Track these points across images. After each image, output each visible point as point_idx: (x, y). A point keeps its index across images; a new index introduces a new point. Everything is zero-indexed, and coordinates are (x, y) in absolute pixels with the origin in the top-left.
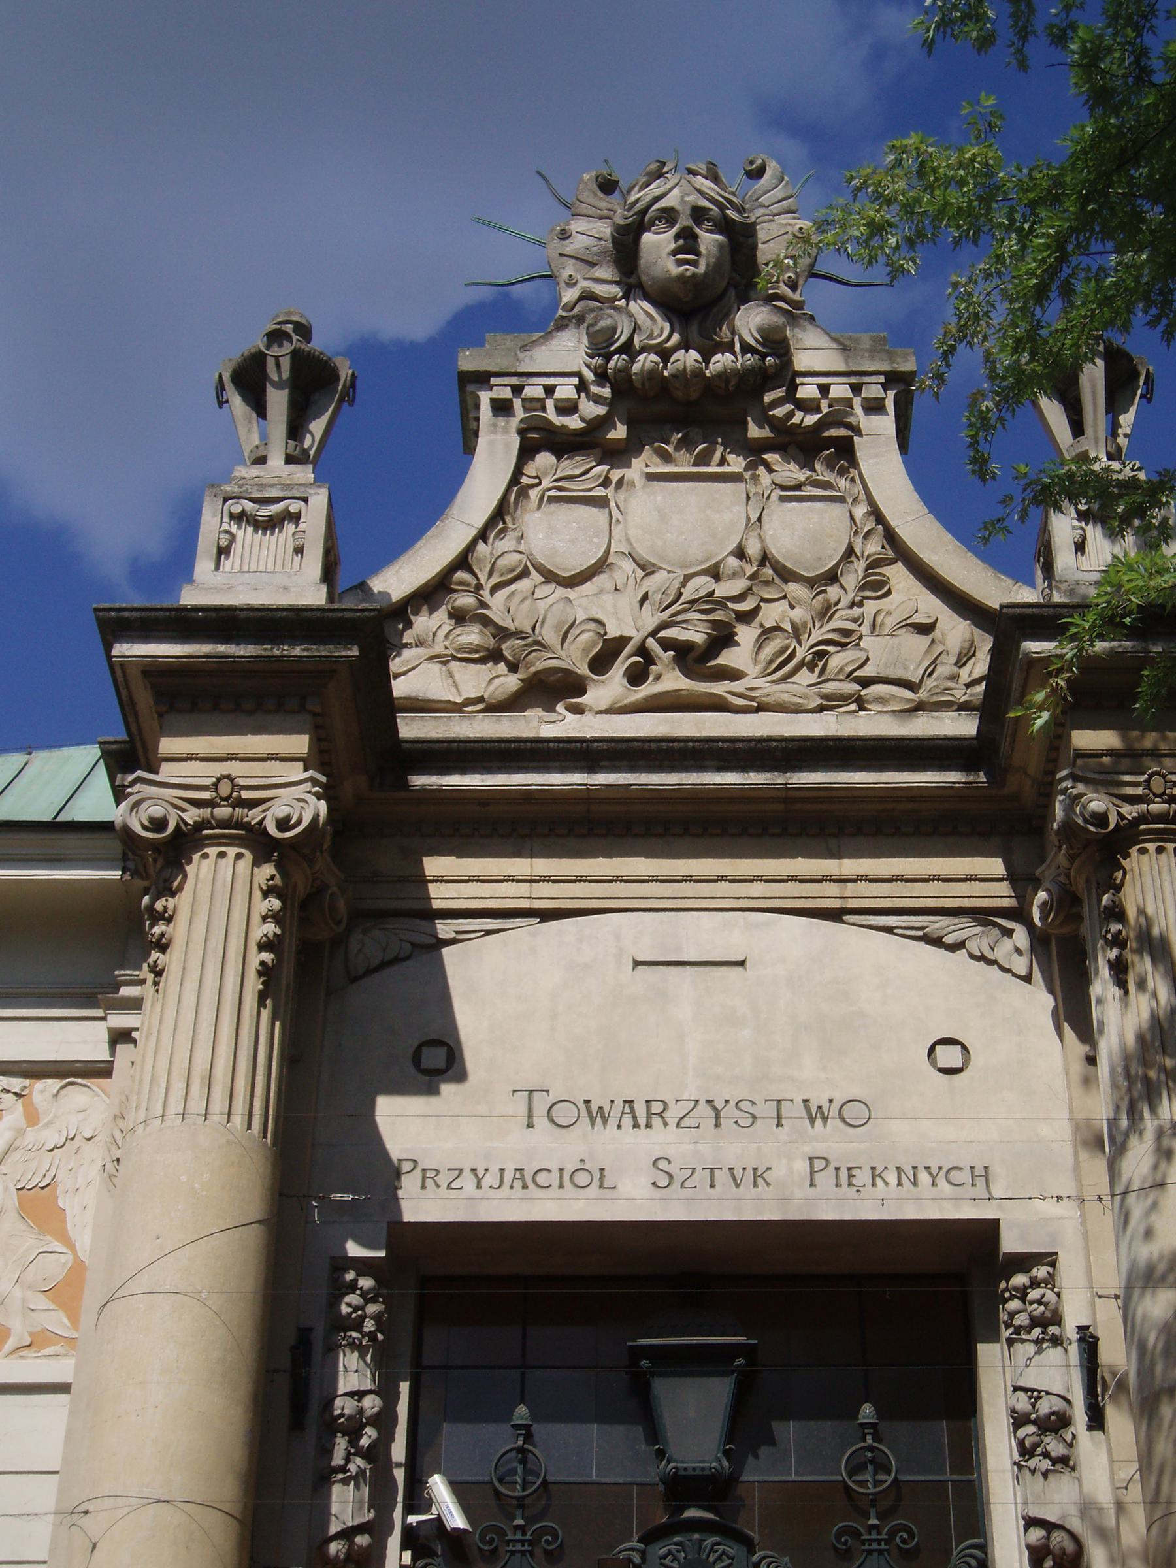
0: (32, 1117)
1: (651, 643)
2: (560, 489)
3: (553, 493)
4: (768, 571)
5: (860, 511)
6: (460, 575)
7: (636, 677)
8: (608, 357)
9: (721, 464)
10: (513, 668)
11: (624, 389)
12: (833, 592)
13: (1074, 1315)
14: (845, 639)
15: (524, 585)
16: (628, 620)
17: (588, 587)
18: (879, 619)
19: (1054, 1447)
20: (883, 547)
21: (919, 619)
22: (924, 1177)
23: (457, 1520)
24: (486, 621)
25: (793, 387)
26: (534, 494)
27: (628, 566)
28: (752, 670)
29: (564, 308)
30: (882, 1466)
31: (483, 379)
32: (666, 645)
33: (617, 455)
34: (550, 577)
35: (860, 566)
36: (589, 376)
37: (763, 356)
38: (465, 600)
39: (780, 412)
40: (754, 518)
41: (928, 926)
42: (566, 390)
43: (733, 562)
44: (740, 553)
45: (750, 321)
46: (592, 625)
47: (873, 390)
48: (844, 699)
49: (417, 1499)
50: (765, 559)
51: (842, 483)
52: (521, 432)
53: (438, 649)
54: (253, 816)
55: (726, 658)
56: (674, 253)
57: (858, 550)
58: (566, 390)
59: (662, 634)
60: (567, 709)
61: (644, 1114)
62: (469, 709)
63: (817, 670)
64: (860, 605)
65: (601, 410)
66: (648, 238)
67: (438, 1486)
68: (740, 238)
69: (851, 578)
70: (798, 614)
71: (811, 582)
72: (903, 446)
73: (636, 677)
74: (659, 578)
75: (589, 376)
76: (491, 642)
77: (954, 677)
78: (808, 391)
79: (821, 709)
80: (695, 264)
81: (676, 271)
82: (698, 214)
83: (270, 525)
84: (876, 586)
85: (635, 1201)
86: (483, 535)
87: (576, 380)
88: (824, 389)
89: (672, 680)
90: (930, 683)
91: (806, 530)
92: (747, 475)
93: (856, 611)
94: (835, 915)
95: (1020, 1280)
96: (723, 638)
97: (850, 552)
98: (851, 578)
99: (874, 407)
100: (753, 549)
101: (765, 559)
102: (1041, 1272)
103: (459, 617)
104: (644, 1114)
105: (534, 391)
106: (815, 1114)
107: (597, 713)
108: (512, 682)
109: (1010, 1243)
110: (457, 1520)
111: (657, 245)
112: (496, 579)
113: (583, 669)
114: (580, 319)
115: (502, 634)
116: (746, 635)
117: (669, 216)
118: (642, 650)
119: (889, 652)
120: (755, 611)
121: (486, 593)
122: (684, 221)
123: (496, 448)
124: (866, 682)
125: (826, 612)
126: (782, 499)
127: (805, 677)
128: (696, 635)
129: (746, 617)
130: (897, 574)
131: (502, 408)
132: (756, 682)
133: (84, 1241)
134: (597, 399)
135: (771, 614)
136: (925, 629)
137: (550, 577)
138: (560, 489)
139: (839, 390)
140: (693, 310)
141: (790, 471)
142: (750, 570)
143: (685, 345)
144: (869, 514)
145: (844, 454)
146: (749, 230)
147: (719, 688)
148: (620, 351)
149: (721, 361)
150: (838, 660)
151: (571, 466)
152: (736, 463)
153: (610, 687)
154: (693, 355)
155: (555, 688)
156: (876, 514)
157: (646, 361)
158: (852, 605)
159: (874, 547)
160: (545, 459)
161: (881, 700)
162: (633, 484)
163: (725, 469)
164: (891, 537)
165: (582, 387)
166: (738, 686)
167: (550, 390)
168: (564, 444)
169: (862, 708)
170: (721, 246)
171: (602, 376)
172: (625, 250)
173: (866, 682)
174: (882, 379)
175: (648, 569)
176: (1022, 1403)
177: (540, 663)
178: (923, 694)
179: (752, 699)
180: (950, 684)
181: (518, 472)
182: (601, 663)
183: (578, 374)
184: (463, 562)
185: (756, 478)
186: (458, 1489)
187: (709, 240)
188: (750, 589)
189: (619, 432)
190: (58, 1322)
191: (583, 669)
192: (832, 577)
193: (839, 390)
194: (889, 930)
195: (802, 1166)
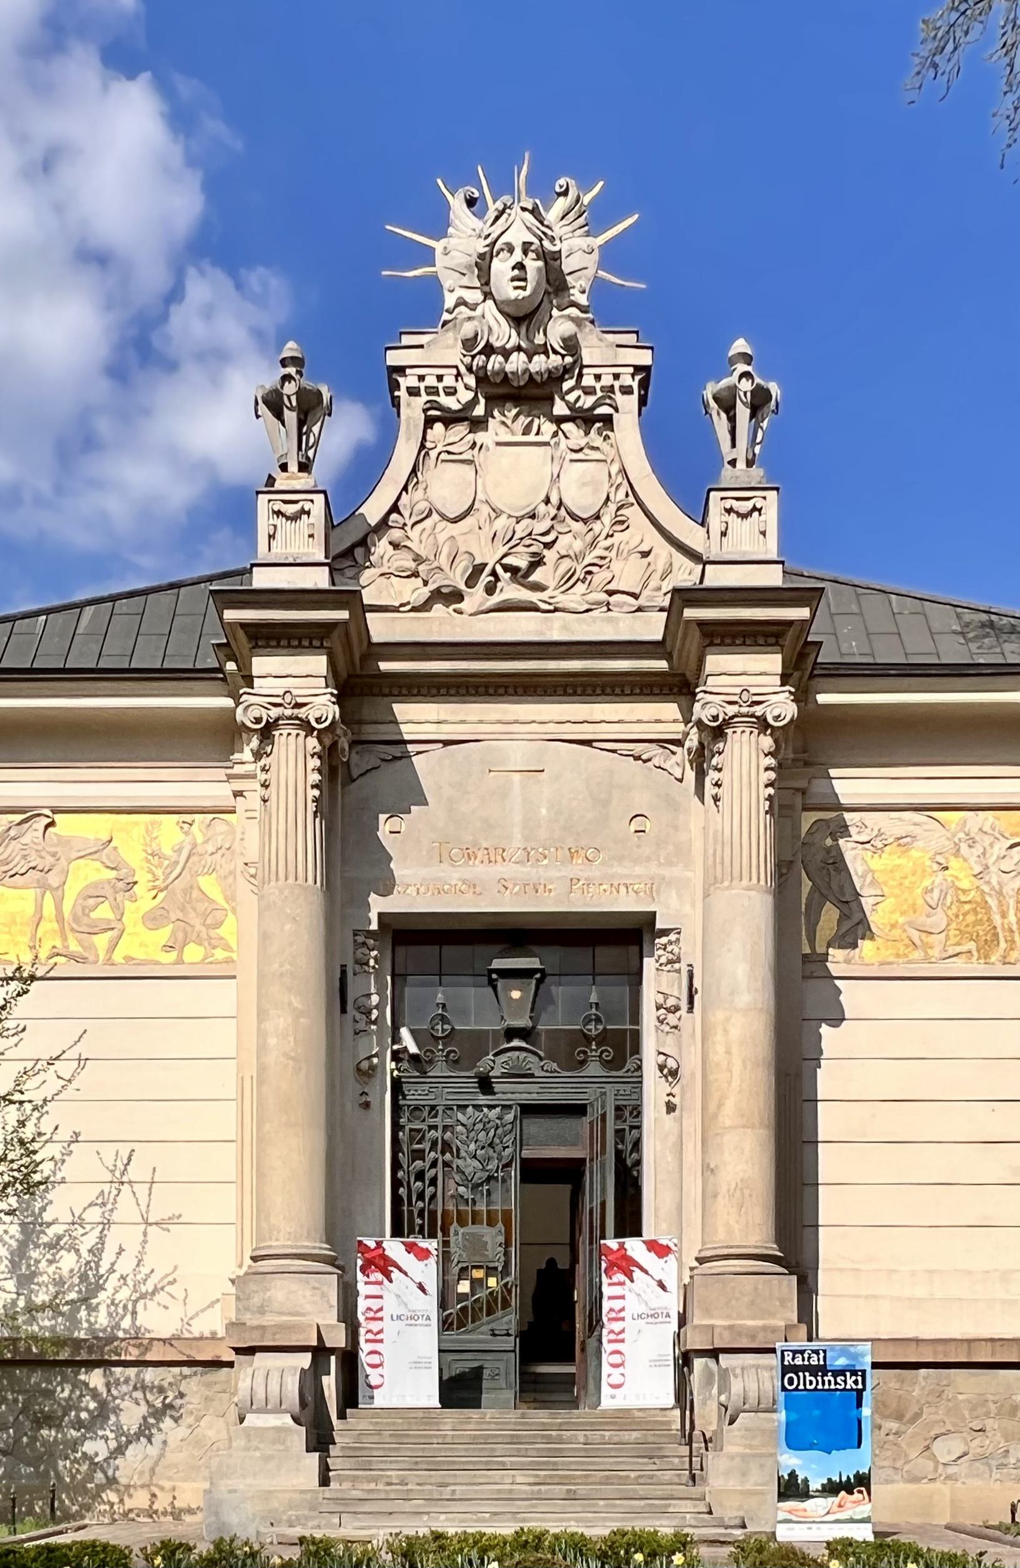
2: (449, 453)
3: (444, 456)
4: (563, 512)
5: (614, 469)
6: (394, 516)
7: (490, 590)
8: (473, 357)
9: (538, 434)
11: (483, 379)
12: (597, 526)
14: (601, 563)
15: (428, 523)
18: (621, 547)
19: (672, 1019)
20: (627, 495)
21: (645, 548)
22: (623, 889)
23: (413, 1049)
25: (580, 375)
26: (433, 454)
27: (485, 510)
28: (552, 584)
29: (447, 311)
30: (598, 1020)
31: (401, 370)
32: (506, 568)
33: (478, 424)
34: (443, 517)
35: (612, 507)
36: (463, 370)
37: (563, 356)
39: (571, 398)
40: (555, 476)
42: (449, 381)
43: (542, 509)
44: (547, 501)
45: (558, 328)
46: (467, 555)
47: (627, 380)
48: (599, 603)
49: (396, 1039)
50: (561, 503)
51: (605, 446)
52: (425, 411)
53: (385, 570)
55: (536, 576)
56: (513, 280)
57: (612, 497)
59: (504, 561)
60: (455, 611)
62: (402, 609)
63: (587, 582)
64: (612, 536)
65: (470, 395)
66: (496, 263)
67: (404, 1032)
68: (551, 260)
69: (607, 519)
70: (578, 545)
71: (585, 521)
72: (640, 414)
73: (490, 590)
74: (501, 523)
75: (463, 370)
76: (413, 565)
77: (659, 589)
78: (588, 381)
79: (587, 611)
80: (524, 288)
81: (514, 294)
82: (526, 247)
84: (620, 523)
86: (405, 488)
87: (454, 371)
88: (598, 377)
89: (510, 591)
90: (645, 593)
92: (552, 443)
93: (610, 541)
94: (588, 743)
95: (664, 940)
96: (537, 562)
97: (608, 499)
98: (607, 519)
99: (627, 391)
100: (554, 500)
101: (561, 503)
102: (673, 937)
103: (396, 546)
105: (431, 381)
107: (471, 615)
108: (425, 592)
110: (413, 1049)
111: (502, 268)
112: (414, 519)
115: (418, 559)
116: (550, 556)
118: (494, 573)
120: (554, 542)
121: (408, 528)
122: (518, 256)
123: (412, 410)
124: (611, 593)
125: (593, 544)
126: (572, 461)
127: (581, 588)
128: (522, 563)
129: (548, 546)
130: (633, 513)
131: (413, 392)
134: (467, 387)
136: (645, 554)
137: (443, 517)
138: (449, 453)
140: (524, 318)
142: (553, 512)
143: (519, 349)
144: (620, 471)
145: (608, 420)
146: (557, 256)
148: (480, 353)
149: (539, 364)
150: (600, 577)
152: (548, 428)
153: (475, 598)
154: (523, 356)
156: (623, 471)
158: (608, 536)
161: (620, 605)
162: (488, 449)
163: (539, 439)
165: (458, 375)
166: (544, 595)
167: (440, 378)
168: (450, 419)
169: (609, 610)
170: (539, 269)
172: (483, 265)
173: (611, 593)
174: (631, 370)
176: (660, 999)
178: (642, 601)
179: (550, 604)
180: (656, 594)
181: (424, 438)
182: (471, 582)
183: (456, 367)
184: (395, 508)
185: (557, 444)
186: (413, 1032)
187: (533, 265)
188: (552, 527)
191: (463, 587)
193: (607, 380)
194: (614, 751)
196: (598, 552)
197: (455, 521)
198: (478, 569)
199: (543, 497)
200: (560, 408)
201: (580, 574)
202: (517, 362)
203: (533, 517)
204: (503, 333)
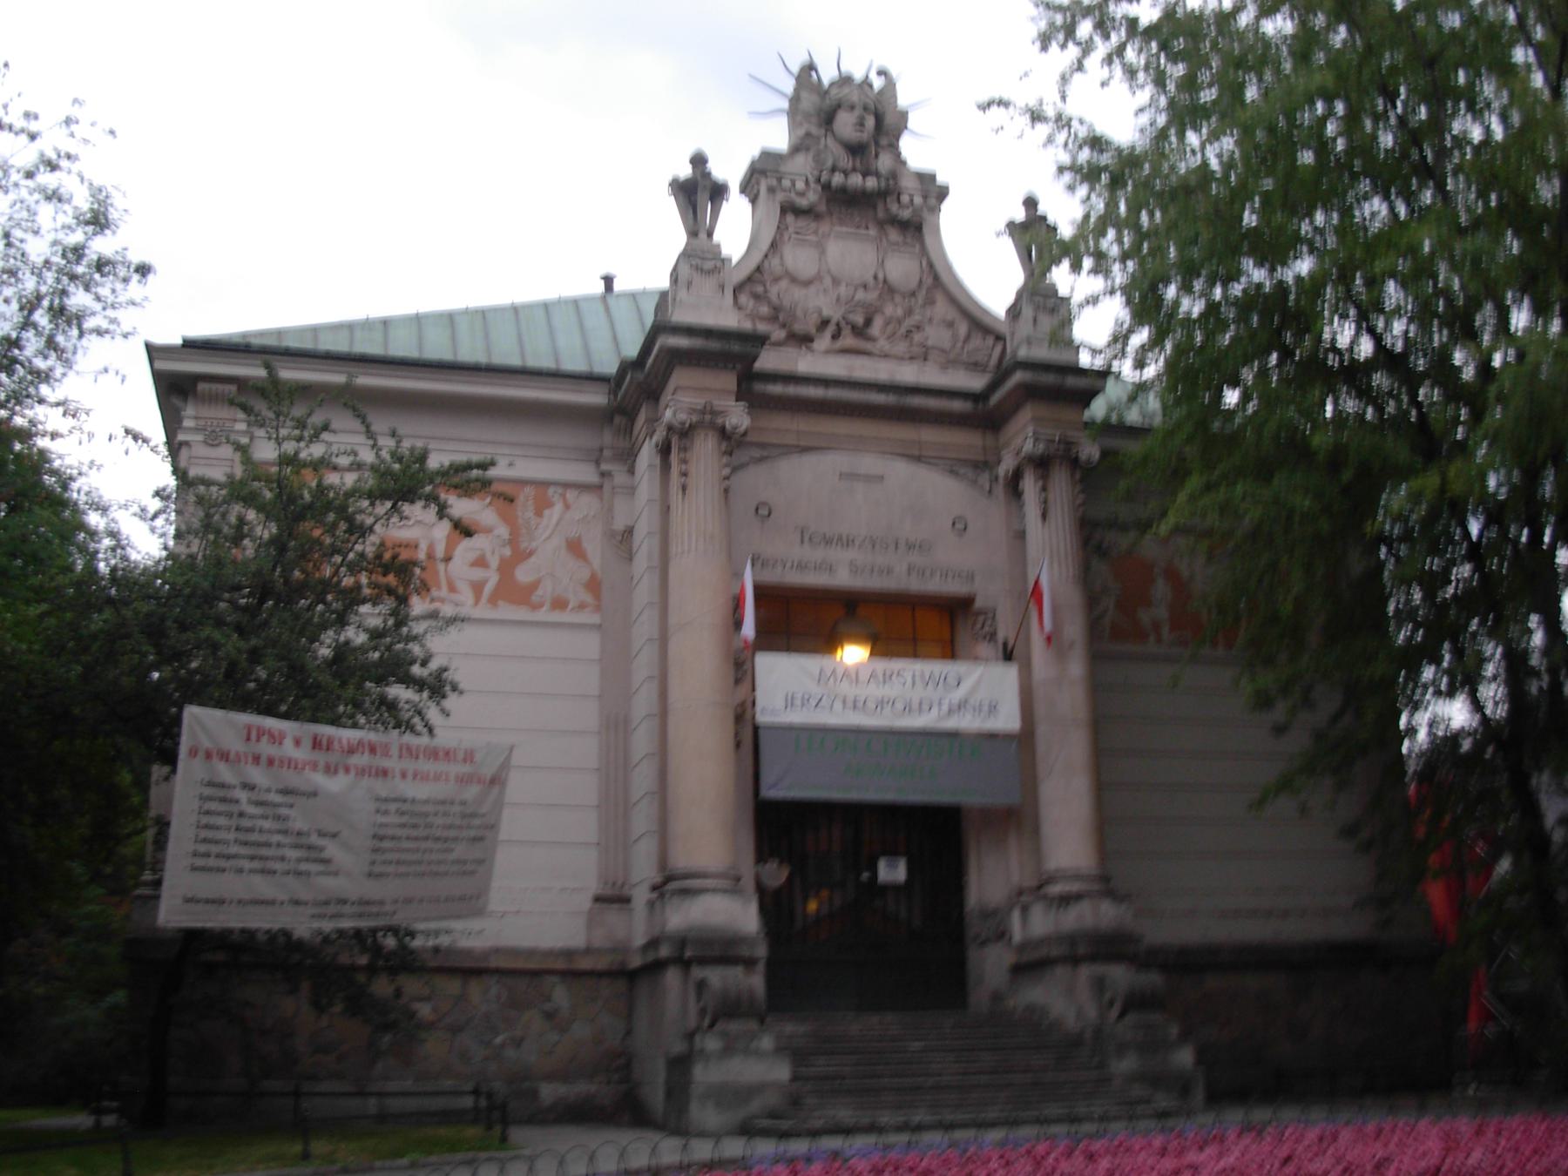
0: (567, 507)
1: (843, 324)
7: (835, 337)
10: (784, 326)
13: (1001, 636)
16: (833, 312)
17: (812, 289)
24: (769, 303)
34: (794, 280)
36: (811, 179)
38: (760, 289)
41: (953, 465)
44: (875, 277)
54: (719, 421)
58: (800, 185)
61: (848, 542)
73: (835, 337)
74: (843, 289)
75: (811, 179)
78: (905, 199)
83: (710, 272)
84: (930, 302)
85: (843, 579)
89: (848, 340)
91: (902, 268)
96: (868, 322)
100: (881, 276)
101: (885, 281)
103: (756, 297)
104: (848, 542)
106: (910, 547)
109: (978, 604)
113: (813, 331)
114: (808, 149)
115: (777, 309)
117: (852, 108)
119: (936, 335)
128: (859, 319)
132: (883, 344)
133: (596, 562)
135: (889, 310)
139: (918, 200)
141: (894, 235)
147: (868, 346)
149: (871, 183)
150: (917, 337)
151: (802, 222)
153: (823, 342)
155: (805, 340)
156: (931, 266)
157: (838, 179)
159: (929, 281)
160: (790, 218)
164: (936, 278)
168: (798, 212)
171: (818, 180)
175: (836, 282)
177: (799, 328)
178: (952, 356)
184: (759, 269)
187: (870, 122)
189: (822, 208)
190: (589, 599)
191: (813, 331)
192: (913, 294)
195: (905, 567)
196: (916, 318)
197: (807, 283)
198: (825, 323)
199: (872, 273)
200: (881, 214)
201: (903, 330)
202: (856, 180)
203: (865, 287)
204: (845, 161)
